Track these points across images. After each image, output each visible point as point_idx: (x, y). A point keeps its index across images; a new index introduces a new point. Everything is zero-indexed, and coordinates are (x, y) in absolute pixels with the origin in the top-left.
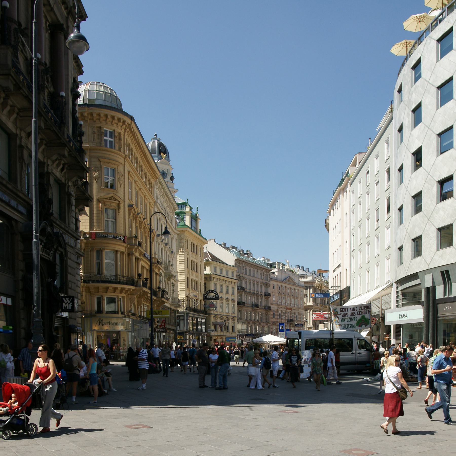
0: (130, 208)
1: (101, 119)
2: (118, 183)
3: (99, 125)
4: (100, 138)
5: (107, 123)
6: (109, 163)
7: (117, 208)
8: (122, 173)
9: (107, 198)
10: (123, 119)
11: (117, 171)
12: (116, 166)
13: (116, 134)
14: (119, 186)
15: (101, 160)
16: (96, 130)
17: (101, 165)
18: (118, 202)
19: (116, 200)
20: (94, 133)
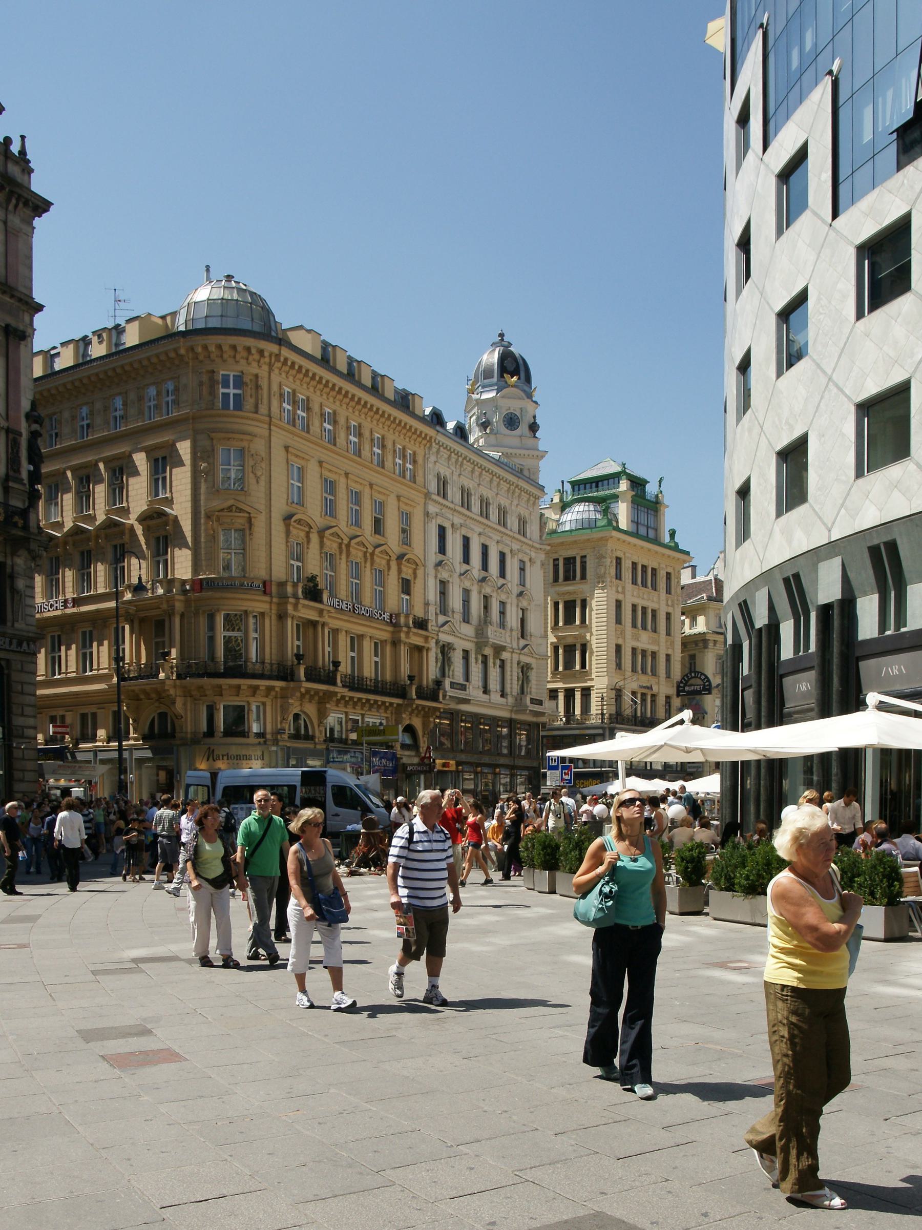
0: (287, 522)
1: (225, 356)
2: (251, 475)
3: (210, 368)
4: (213, 392)
5: (224, 361)
6: (229, 439)
7: (247, 525)
8: (263, 454)
9: (222, 510)
10: (255, 347)
11: (249, 451)
12: (245, 444)
13: (246, 379)
14: (252, 480)
15: (213, 435)
16: (205, 378)
17: (213, 446)
18: (247, 515)
19: (241, 510)
20: (201, 384)
